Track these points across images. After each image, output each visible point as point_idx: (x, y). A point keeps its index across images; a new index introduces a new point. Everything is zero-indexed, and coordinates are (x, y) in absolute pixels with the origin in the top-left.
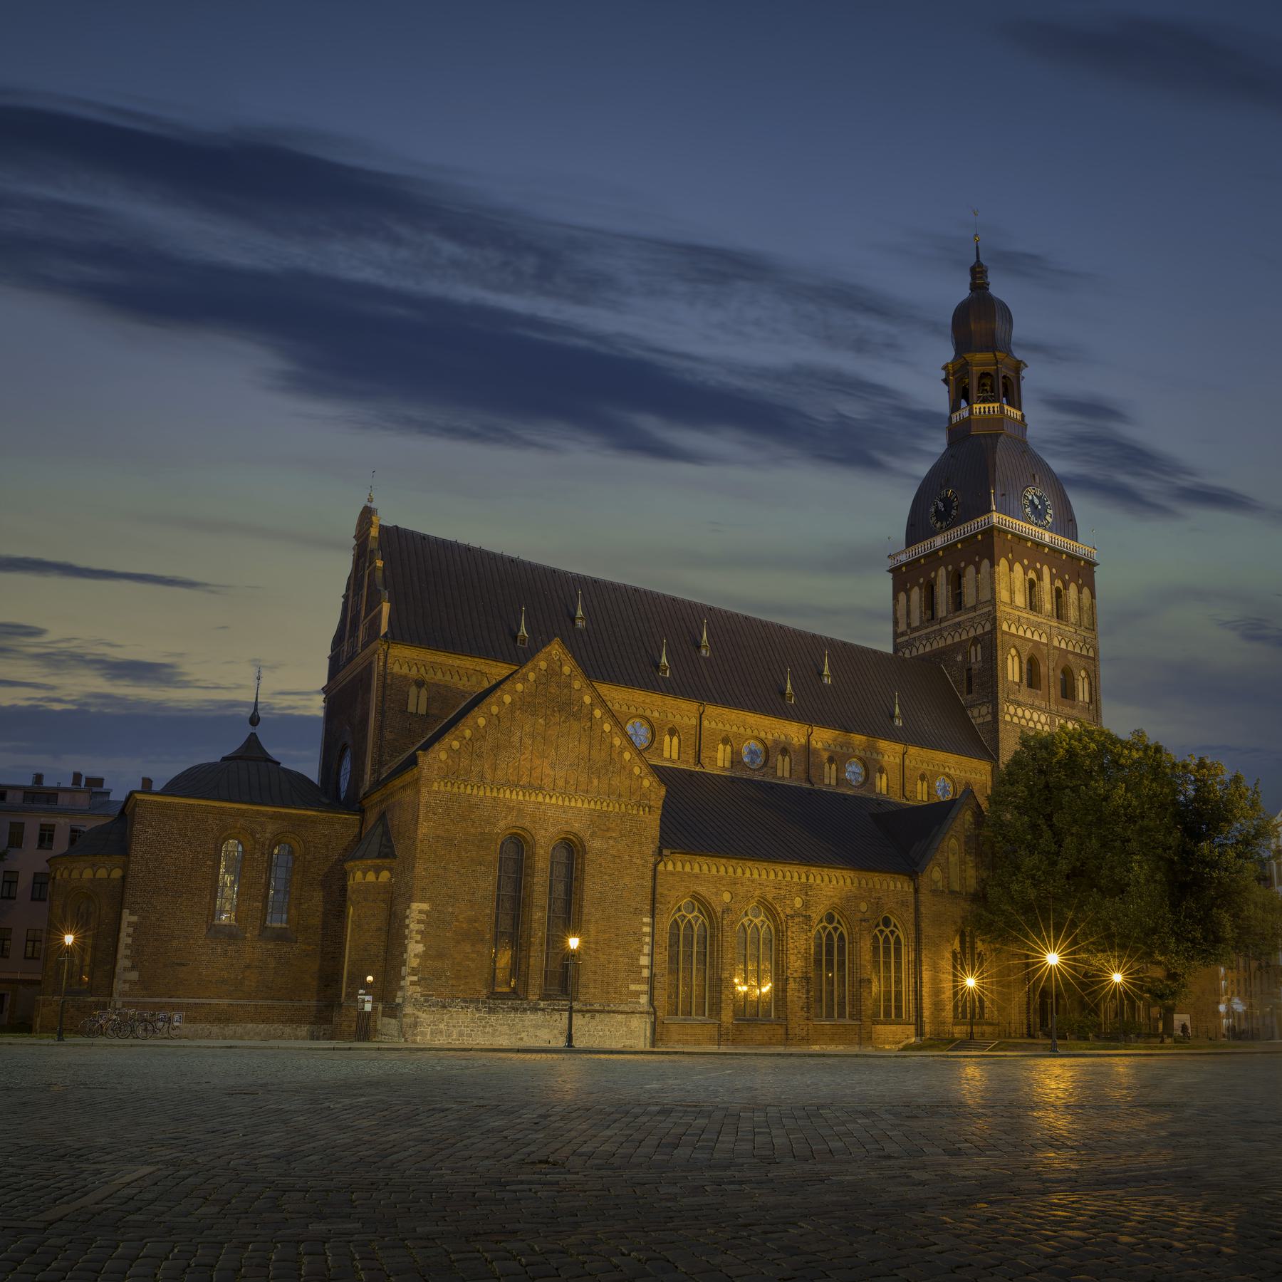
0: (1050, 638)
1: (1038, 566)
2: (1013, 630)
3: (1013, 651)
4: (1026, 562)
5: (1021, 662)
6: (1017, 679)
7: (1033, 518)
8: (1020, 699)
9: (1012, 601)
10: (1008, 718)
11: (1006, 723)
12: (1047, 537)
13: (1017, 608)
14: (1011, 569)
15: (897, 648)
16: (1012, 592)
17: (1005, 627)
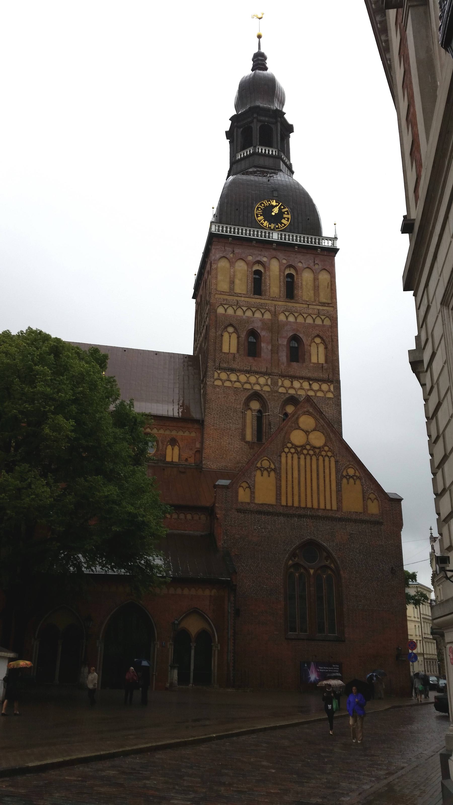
0: (275, 314)
1: (265, 259)
2: (230, 311)
3: (231, 329)
4: (250, 258)
5: (238, 338)
6: (234, 350)
7: (266, 223)
8: (235, 366)
9: (232, 288)
10: (218, 383)
11: (215, 387)
12: (275, 236)
13: (237, 295)
14: (232, 263)
15: (194, 353)
16: (232, 282)
17: (221, 310)
